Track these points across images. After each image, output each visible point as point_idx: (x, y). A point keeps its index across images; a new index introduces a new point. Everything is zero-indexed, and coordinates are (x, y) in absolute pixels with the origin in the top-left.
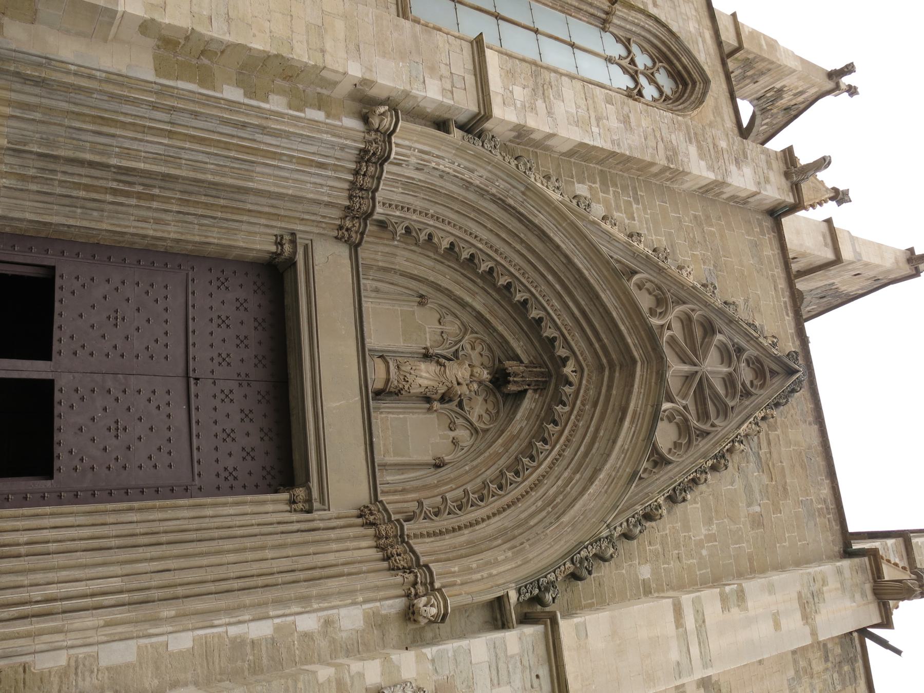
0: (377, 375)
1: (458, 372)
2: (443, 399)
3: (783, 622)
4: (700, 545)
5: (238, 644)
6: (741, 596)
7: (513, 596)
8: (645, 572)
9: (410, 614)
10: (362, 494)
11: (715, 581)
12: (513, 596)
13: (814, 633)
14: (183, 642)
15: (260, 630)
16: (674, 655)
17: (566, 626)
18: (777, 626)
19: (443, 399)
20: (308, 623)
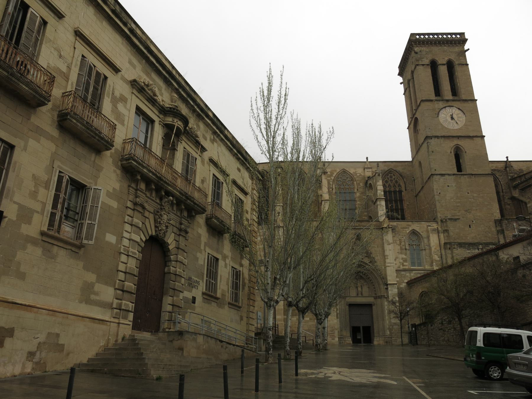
0: (360, 295)
1: (359, 284)
2: (361, 286)
3: (390, 249)
4: (380, 258)
5: (387, 313)
6: (387, 256)
7: (385, 287)
8: (383, 267)
9: (386, 298)
10: (373, 298)
11: (385, 259)
12: (385, 287)
13: (392, 243)
14: (387, 317)
15: (386, 311)
16: (392, 268)
17: (389, 283)
18: (390, 250)
19: (361, 286)
20: (386, 307)
